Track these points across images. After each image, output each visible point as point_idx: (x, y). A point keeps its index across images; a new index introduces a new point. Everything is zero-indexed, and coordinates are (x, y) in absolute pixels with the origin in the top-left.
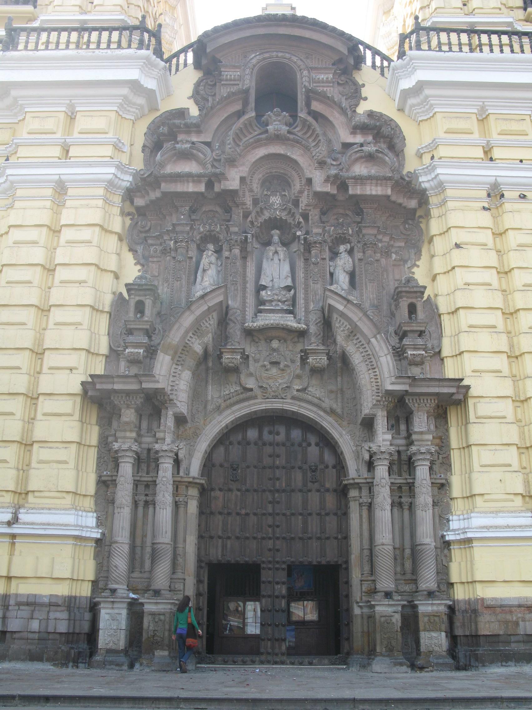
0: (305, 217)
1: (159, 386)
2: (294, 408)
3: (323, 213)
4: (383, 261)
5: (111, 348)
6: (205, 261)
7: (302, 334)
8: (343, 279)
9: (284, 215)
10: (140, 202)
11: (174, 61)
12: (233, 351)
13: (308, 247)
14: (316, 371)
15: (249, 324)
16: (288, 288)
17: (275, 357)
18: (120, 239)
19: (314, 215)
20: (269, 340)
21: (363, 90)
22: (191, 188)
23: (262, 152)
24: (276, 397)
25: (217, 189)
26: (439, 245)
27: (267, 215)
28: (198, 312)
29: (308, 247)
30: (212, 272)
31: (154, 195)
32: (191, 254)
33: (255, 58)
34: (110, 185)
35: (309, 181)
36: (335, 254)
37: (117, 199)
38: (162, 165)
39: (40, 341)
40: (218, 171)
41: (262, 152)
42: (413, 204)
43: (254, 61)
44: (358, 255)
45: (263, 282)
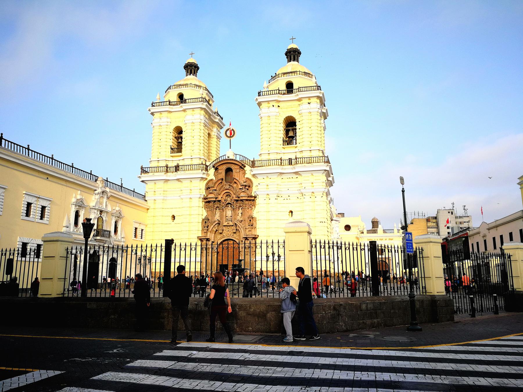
1: (208, 238)
2: (232, 239)
4: (247, 210)
5: (202, 229)
6: (216, 213)
8: (240, 215)
10: (205, 201)
11: (210, 165)
13: (234, 209)
14: (234, 233)
16: (231, 216)
17: (228, 230)
19: (235, 202)
21: (246, 171)
22: (213, 199)
24: (228, 237)
27: (227, 202)
28: (214, 225)
29: (234, 209)
30: (218, 214)
31: (207, 200)
32: (214, 211)
33: (225, 167)
34: (200, 198)
35: (233, 197)
37: (201, 200)
38: (208, 196)
40: (217, 197)
42: (253, 198)
43: (224, 168)
44: (243, 210)
45: (227, 216)
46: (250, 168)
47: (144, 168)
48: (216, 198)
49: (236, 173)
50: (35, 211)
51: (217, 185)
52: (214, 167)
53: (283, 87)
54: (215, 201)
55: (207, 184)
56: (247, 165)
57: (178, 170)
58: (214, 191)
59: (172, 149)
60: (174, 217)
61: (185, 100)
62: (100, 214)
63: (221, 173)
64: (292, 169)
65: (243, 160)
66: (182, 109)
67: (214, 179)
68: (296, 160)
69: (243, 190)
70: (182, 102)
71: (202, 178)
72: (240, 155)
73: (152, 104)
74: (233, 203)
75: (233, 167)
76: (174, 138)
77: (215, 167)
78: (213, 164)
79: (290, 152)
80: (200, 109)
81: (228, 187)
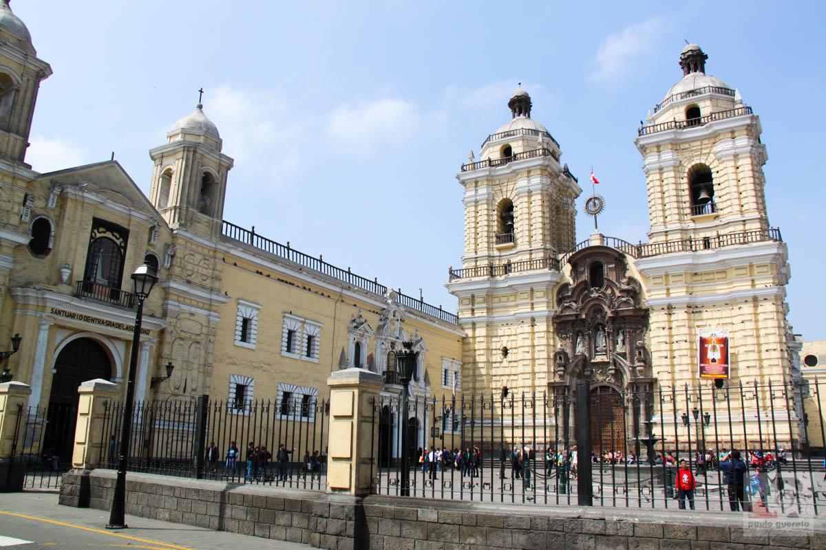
0: (607, 322)
3: (613, 321)
6: (579, 340)
7: (609, 362)
9: (602, 322)
10: (558, 321)
12: (588, 371)
15: (593, 361)
16: (604, 347)
18: (553, 332)
20: (599, 365)
22: (571, 318)
23: (591, 304)
25: (579, 318)
26: (652, 326)
27: (596, 322)
33: (588, 261)
36: (618, 335)
37: (551, 319)
39: (533, 370)
41: (591, 304)
42: (643, 313)
46: (634, 260)
47: (454, 271)
48: (577, 316)
49: (609, 272)
50: (300, 343)
51: (576, 293)
52: (569, 261)
53: (682, 117)
54: (573, 322)
55: (559, 292)
56: (628, 253)
57: (510, 271)
58: (574, 304)
59: (497, 237)
60: (505, 352)
61: (515, 156)
62: (391, 346)
63: (583, 272)
64: (713, 255)
65: (620, 246)
66: (508, 171)
67: (571, 282)
68: (719, 238)
69: (624, 299)
70: (510, 160)
71: (551, 281)
72: (614, 239)
73: (462, 168)
74: (607, 322)
75: (602, 260)
76: (499, 220)
77: (572, 262)
78: (568, 257)
79: (704, 226)
80: (539, 167)
81: (595, 295)
